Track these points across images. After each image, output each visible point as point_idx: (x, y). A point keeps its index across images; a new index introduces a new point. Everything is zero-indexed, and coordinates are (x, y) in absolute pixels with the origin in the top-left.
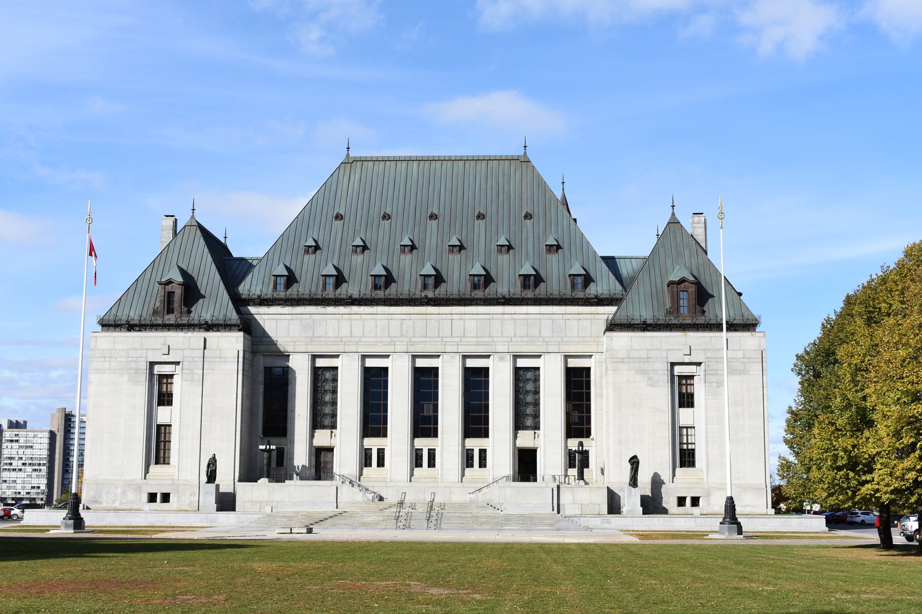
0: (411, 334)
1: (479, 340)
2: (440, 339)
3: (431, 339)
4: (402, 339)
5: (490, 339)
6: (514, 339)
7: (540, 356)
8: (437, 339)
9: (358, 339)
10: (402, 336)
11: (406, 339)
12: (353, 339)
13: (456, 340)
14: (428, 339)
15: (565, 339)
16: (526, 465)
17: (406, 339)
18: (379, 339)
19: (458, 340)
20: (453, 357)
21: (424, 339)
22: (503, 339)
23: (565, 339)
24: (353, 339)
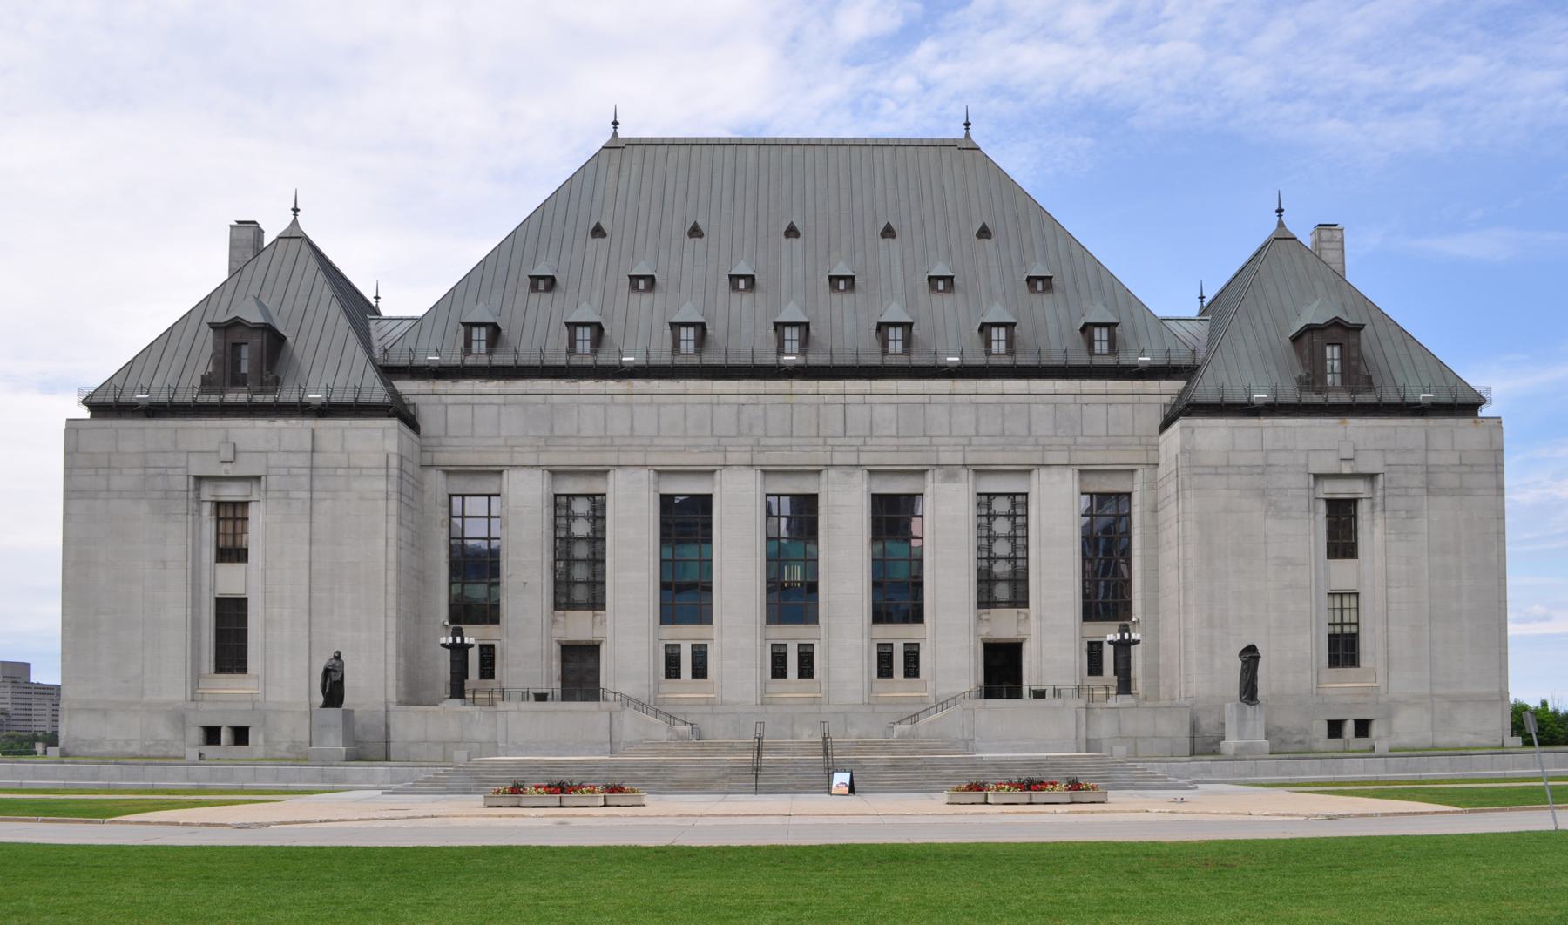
0: (759, 431)
1: (902, 441)
2: (821, 441)
3: (801, 441)
4: (742, 440)
5: (926, 441)
6: (975, 441)
7: (1029, 472)
8: (815, 441)
9: (647, 442)
10: (739, 434)
11: (750, 441)
12: (637, 442)
13: (854, 441)
14: (794, 441)
15: (1080, 440)
16: (1002, 669)
17: (750, 441)
18: (690, 442)
19: (861, 441)
20: (848, 474)
21: (787, 441)
22: (953, 441)
23: (1080, 440)
24: (637, 442)
